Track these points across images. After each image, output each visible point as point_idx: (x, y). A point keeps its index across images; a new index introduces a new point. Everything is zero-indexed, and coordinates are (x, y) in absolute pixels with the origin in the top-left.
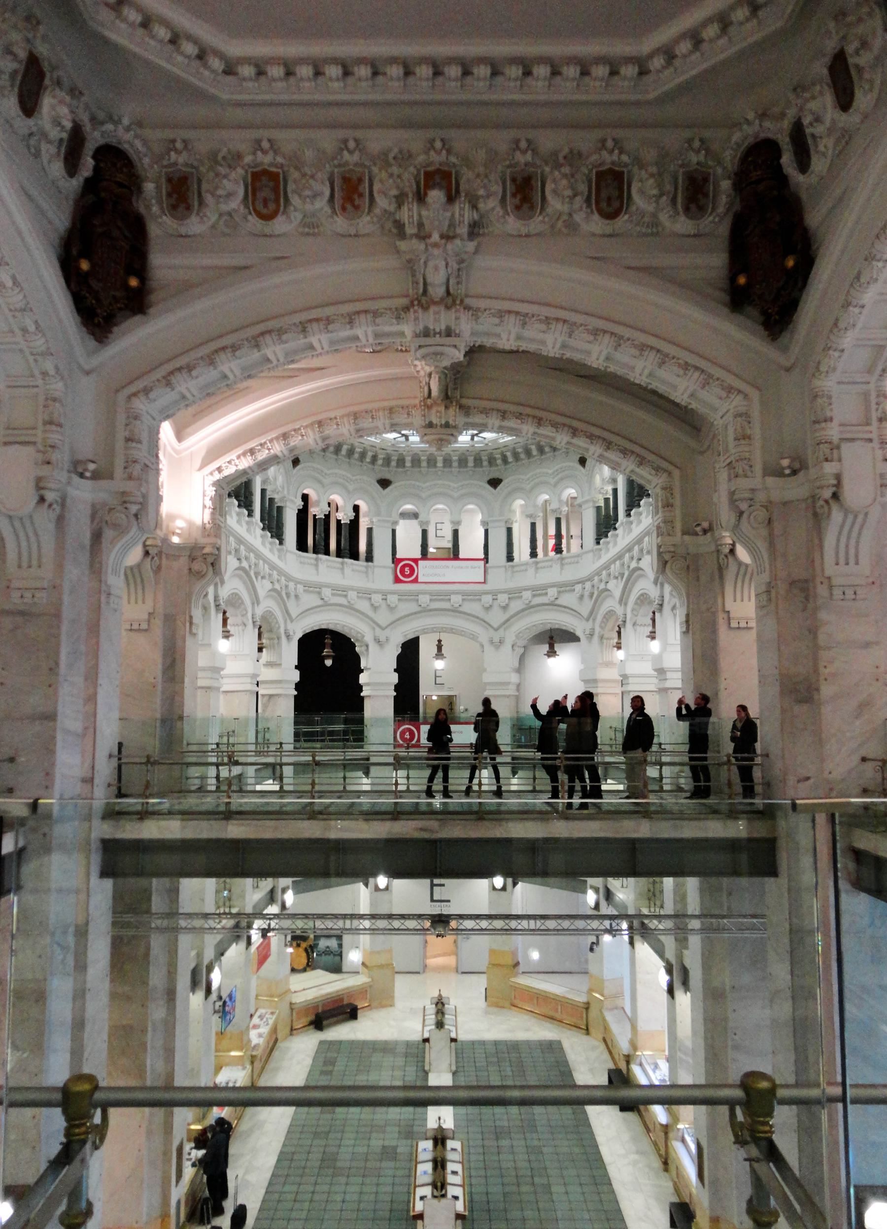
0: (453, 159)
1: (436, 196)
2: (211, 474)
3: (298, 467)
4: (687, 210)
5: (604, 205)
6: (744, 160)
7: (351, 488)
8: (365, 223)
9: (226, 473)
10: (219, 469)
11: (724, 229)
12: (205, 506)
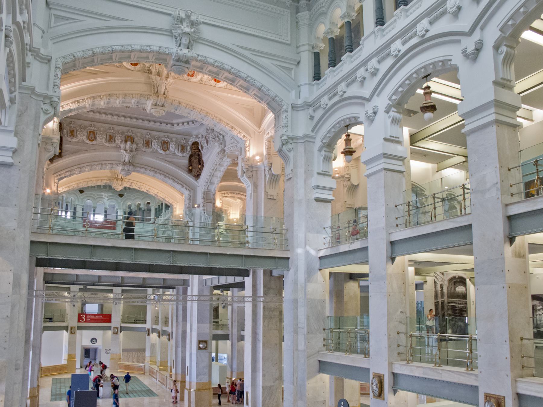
0: (133, 135)
1: (129, 144)
4: (181, 151)
5: (164, 148)
6: (192, 144)
8: (113, 145)
11: (188, 156)
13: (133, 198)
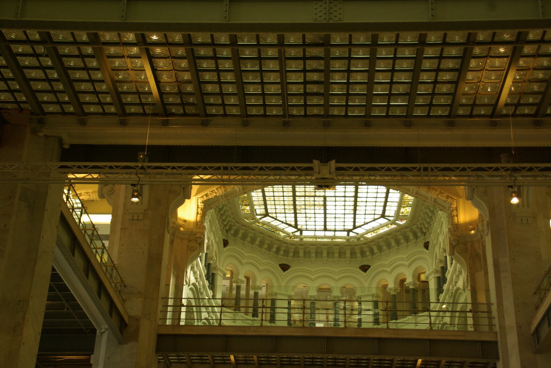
2: (202, 197)
3: (226, 248)
7: (262, 268)
9: (210, 197)
10: (207, 195)
12: (198, 213)
13: (389, 270)
